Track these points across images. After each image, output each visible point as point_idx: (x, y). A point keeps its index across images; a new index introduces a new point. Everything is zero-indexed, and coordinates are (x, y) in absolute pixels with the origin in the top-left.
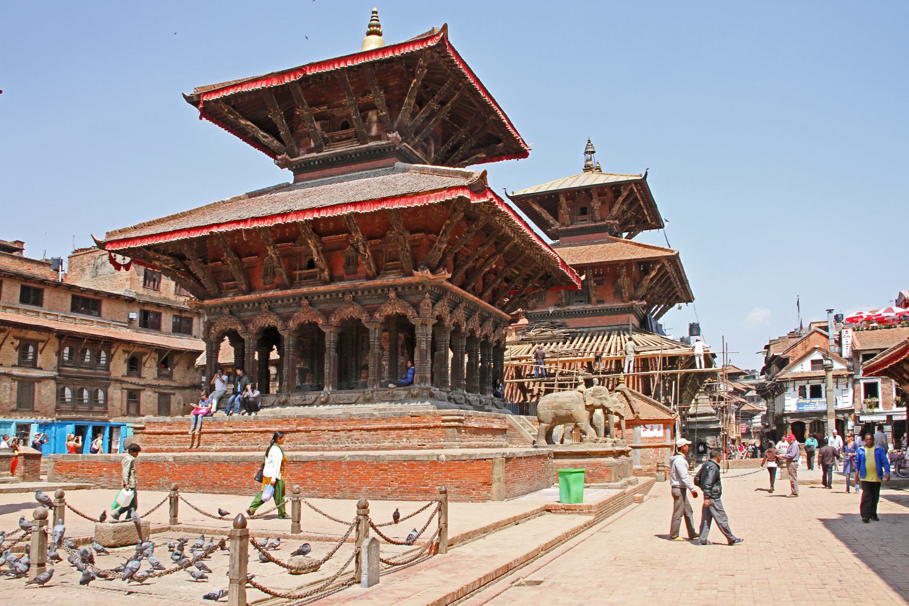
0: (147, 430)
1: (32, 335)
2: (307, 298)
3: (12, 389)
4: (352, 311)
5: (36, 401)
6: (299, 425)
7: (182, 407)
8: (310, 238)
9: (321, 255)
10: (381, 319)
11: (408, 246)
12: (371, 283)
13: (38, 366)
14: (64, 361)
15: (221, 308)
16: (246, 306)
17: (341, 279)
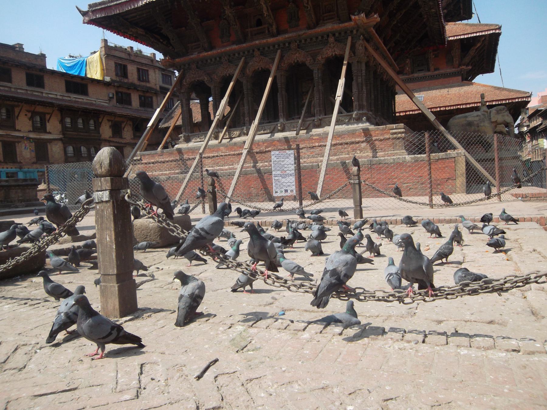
0: (144, 161)
1: (40, 109)
2: (259, 49)
4: (297, 56)
5: (50, 156)
6: (266, 147)
9: (270, 11)
10: (323, 62)
12: (310, 32)
13: (48, 131)
14: (68, 128)
15: (189, 65)
16: (209, 61)
17: (286, 32)
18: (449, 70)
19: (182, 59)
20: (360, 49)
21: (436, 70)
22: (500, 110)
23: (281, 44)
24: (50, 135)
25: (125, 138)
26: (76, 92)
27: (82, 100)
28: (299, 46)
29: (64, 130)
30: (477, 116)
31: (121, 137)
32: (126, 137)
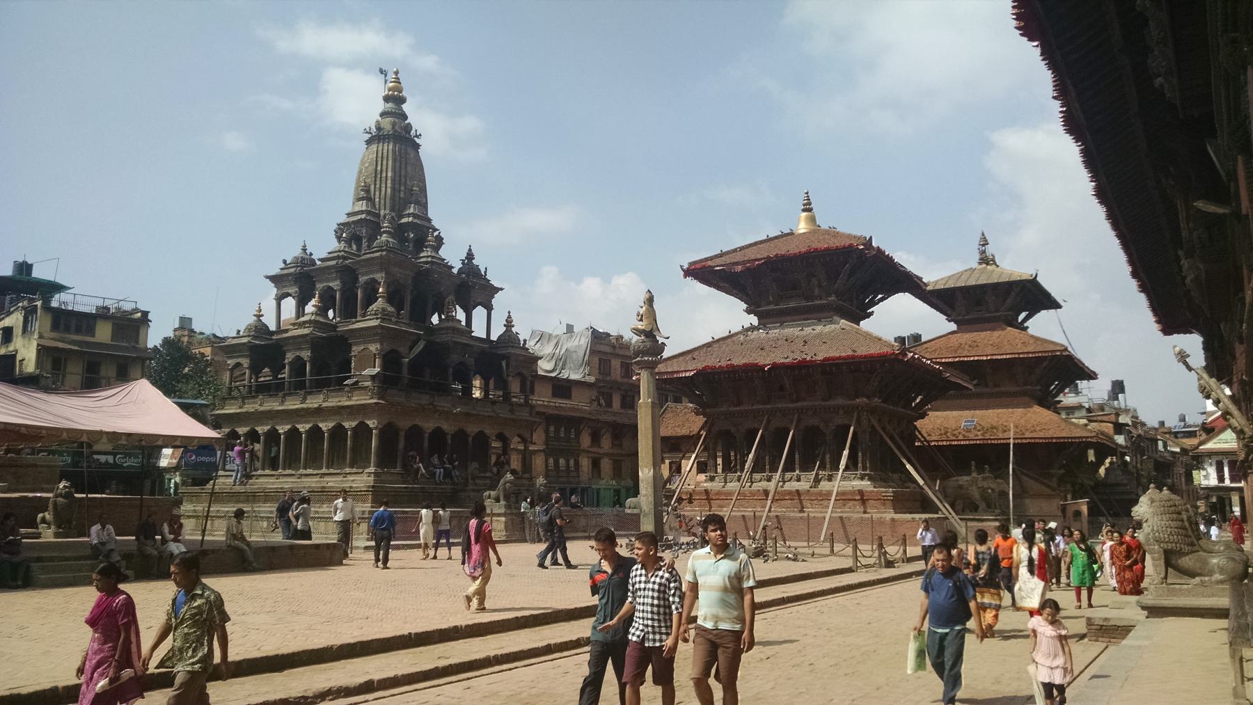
3: (518, 460)
4: (815, 421)
5: (533, 470)
7: (630, 471)
16: (736, 414)
21: (997, 386)
25: (603, 448)
26: (561, 397)
27: (565, 405)
29: (547, 442)
30: (967, 481)
31: (599, 446)
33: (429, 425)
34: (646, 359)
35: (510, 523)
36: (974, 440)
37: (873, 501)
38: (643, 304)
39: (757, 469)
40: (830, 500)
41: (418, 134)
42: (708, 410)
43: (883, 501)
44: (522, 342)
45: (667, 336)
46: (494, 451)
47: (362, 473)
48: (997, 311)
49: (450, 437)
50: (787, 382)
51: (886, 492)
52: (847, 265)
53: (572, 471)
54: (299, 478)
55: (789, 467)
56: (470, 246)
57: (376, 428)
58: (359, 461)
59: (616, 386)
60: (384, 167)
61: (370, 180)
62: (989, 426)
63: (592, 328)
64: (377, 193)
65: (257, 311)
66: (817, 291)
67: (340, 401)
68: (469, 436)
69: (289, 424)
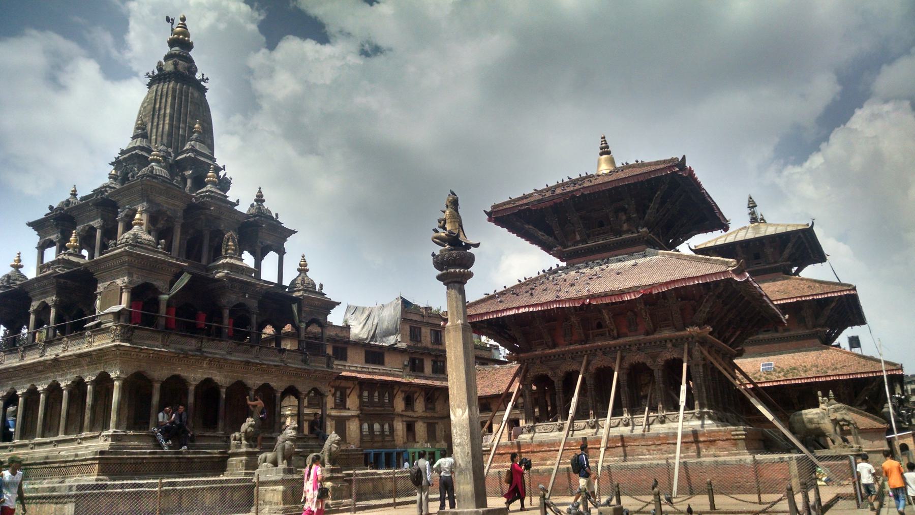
2: (601, 349)
3: (331, 427)
4: (638, 358)
5: (347, 435)
7: (443, 433)
8: (604, 309)
9: (612, 321)
10: (662, 363)
11: (679, 310)
13: (347, 407)
14: (365, 402)
16: (552, 357)
18: (801, 332)
19: (527, 355)
20: (696, 353)
22: (838, 408)
23: (622, 346)
24: (349, 411)
25: (417, 411)
26: (374, 363)
28: (639, 349)
30: (817, 413)
31: (413, 411)
32: (417, 410)
33: (194, 376)
34: (452, 270)
35: (290, 493)
36: (777, 381)
37: (721, 443)
38: (445, 208)
39: (581, 414)
40: (676, 444)
41: (205, 78)
42: (522, 355)
43: (734, 441)
44: (318, 288)
45: (476, 242)
46: (306, 418)
47: (98, 437)
48: (775, 262)
49: (224, 390)
50: (607, 317)
51: (736, 431)
52: (659, 193)
53: (387, 436)
54: (32, 448)
55: (617, 412)
56: (260, 188)
57: (118, 378)
58: (100, 422)
59: (426, 352)
60: (163, 105)
61: (147, 118)
62: (788, 368)
63: (401, 298)
64: (154, 131)
65: (15, 261)
66: (625, 227)
67: (80, 349)
68: (250, 389)
69: (29, 382)
